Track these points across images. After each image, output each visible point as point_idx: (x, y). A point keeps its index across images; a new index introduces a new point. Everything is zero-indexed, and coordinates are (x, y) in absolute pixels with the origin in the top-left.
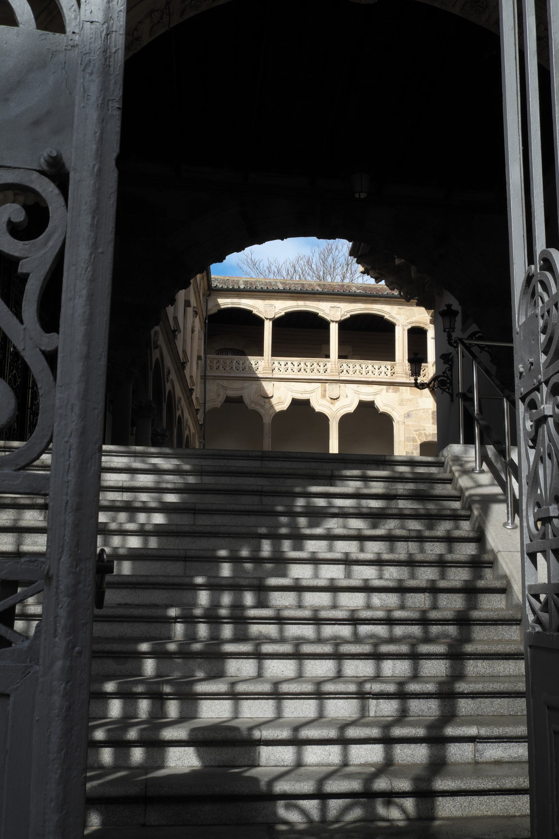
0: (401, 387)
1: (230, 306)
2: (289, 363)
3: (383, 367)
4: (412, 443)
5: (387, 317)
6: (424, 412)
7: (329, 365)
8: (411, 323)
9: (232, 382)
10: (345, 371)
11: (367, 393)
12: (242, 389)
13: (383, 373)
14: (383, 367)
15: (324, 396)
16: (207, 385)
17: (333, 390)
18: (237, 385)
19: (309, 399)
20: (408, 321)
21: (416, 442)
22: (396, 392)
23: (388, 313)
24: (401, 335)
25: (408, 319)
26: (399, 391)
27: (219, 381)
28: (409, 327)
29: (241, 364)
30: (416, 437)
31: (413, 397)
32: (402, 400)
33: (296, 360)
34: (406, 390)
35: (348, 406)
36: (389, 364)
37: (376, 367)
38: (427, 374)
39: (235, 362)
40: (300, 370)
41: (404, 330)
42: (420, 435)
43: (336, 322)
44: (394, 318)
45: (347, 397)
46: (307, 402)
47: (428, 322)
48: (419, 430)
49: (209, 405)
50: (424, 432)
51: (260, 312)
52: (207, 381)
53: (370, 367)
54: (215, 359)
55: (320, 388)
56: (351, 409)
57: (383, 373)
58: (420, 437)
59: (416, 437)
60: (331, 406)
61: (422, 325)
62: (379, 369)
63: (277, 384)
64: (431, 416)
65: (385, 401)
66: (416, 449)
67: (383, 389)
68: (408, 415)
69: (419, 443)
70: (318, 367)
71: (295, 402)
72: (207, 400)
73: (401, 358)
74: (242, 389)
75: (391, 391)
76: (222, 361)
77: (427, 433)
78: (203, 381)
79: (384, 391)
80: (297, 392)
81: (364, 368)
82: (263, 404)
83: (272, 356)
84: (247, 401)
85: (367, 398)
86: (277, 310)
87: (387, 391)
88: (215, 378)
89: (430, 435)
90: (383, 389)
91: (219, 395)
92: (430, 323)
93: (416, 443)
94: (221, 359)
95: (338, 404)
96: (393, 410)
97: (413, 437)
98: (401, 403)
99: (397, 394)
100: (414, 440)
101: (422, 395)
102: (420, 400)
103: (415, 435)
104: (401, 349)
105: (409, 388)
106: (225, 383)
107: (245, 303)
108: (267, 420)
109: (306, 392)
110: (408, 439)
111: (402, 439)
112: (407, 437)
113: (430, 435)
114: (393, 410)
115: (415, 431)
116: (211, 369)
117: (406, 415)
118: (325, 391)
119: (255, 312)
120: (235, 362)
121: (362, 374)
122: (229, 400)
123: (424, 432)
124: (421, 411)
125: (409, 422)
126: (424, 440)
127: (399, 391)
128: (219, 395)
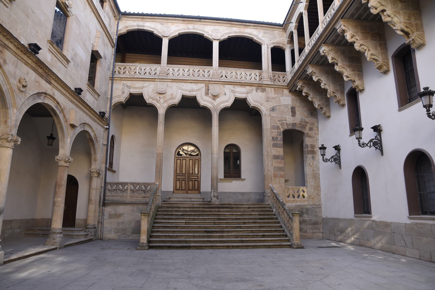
0: (267, 88)
1: (136, 28)
2: (181, 70)
3: (253, 74)
4: (276, 130)
5: (255, 38)
6: (285, 107)
7: (211, 71)
8: (273, 43)
9: (134, 82)
10: (224, 76)
11: (240, 92)
12: (142, 88)
13: (253, 78)
14: (253, 74)
15: (207, 94)
16: (114, 85)
17: (215, 89)
18: (138, 84)
19: (196, 96)
20: (271, 42)
21: (280, 129)
22: (263, 92)
23: (256, 36)
24: (266, 51)
25: (271, 41)
26: (265, 91)
27: (124, 82)
28: (272, 46)
29: (143, 69)
30: (280, 125)
31: (276, 96)
32: (268, 98)
33: (186, 68)
34: (271, 90)
35: (227, 101)
36: (257, 72)
37: (248, 74)
38: (286, 80)
39: (138, 68)
40: (189, 74)
41: (268, 48)
42: (282, 124)
43: (218, 40)
44: (261, 39)
45: (225, 94)
46: (194, 99)
47: (286, 42)
48: (282, 120)
49: (115, 100)
50: (286, 122)
51: (159, 32)
52: (114, 81)
53: (243, 73)
54: (122, 65)
55: (204, 88)
56: (229, 104)
57: (253, 78)
58: (283, 126)
59: (280, 125)
60: (213, 101)
61: (281, 45)
62: (250, 75)
63: (170, 84)
64: (290, 110)
65: (254, 99)
66: (280, 135)
67: (253, 89)
68: (273, 109)
69: (282, 130)
70: (203, 73)
71: (184, 98)
72: (114, 95)
73: (266, 67)
74: (142, 88)
75: (259, 91)
76: (128, 67)
77: (288, 123)
78: (111, 81)
79: (254, 91)
80: (186, 90)
81: (239, 74)
82: (159, 99)
83: (168, 63)
84: (146, 97)
85: (241, 96)
86: (172, 31)
87: (256, 91)
88: (121, 79)
89: (290, 124)
90: (253, 89)
91: (123, 93)
92: (288, 44)
93: (279, 131)
94: (128, 66)
95: (218, 100)
96: (262, 105)
97: (278, 126)
98: (268, 100)
99: (264, 94)
100: (278, 128)
101: (283, 94)
102: (281, 98)
103: (278, 124)
104: (266, 61)
105: (273, 89)
106: (129, 83)
107: (148, 25)
108: (162, 111)
109: (193, 91)
110: (273, 127)
111: (269, 127)
112: (273, 126)
113: (290, 124)
114: (262, 105)
115: (279, 121)
116: (119, 73)
117: (271, 109)
118: (208, 90)
119: (155, 32)
120: (138, 68)
121: (237, 78)
122: (132, 95)
123: (286, 122)
124: (283, 106)
125: (274, 114)
126: (286, 128)
127: (265, 91)
128: (123, 93)
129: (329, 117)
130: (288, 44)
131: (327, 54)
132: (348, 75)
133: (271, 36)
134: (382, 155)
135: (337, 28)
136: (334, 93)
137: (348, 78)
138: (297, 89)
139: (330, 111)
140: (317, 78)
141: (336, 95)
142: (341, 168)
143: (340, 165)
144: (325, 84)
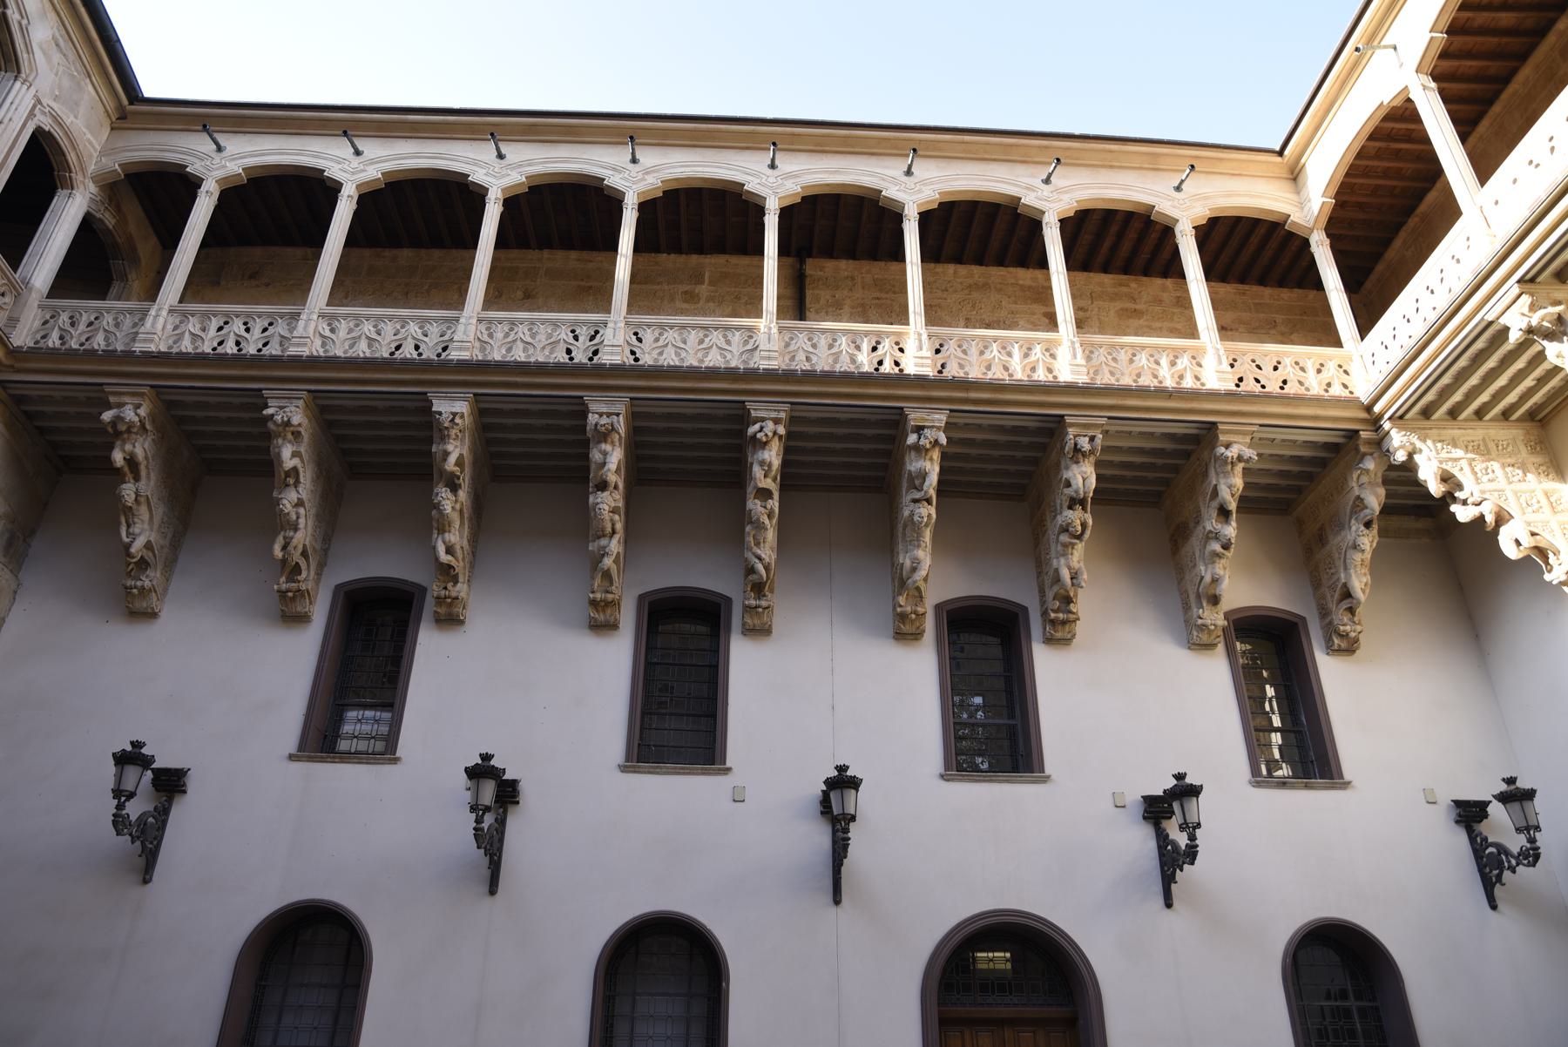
47: (92, 168)
129: (152, 615)
130: (95, 179)
131: (453, 432)
132: (458, 548)
133: (66, 83)
134: (493, 888)
135: (593, 407)
136: (304, 554)
137: (450, 558)
138: (107, 416)
139: (165, 590)
140: (296, 462)
141: (303, 565)
142: (146, 880)
143: (149, 857)
144: (300, 503)
